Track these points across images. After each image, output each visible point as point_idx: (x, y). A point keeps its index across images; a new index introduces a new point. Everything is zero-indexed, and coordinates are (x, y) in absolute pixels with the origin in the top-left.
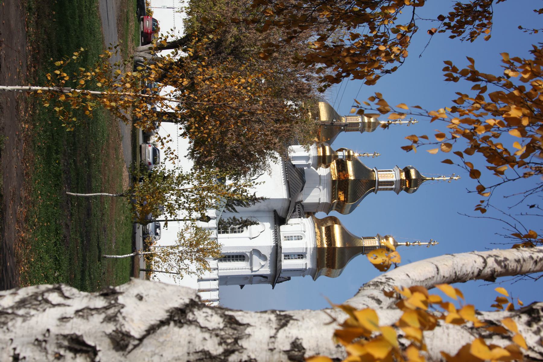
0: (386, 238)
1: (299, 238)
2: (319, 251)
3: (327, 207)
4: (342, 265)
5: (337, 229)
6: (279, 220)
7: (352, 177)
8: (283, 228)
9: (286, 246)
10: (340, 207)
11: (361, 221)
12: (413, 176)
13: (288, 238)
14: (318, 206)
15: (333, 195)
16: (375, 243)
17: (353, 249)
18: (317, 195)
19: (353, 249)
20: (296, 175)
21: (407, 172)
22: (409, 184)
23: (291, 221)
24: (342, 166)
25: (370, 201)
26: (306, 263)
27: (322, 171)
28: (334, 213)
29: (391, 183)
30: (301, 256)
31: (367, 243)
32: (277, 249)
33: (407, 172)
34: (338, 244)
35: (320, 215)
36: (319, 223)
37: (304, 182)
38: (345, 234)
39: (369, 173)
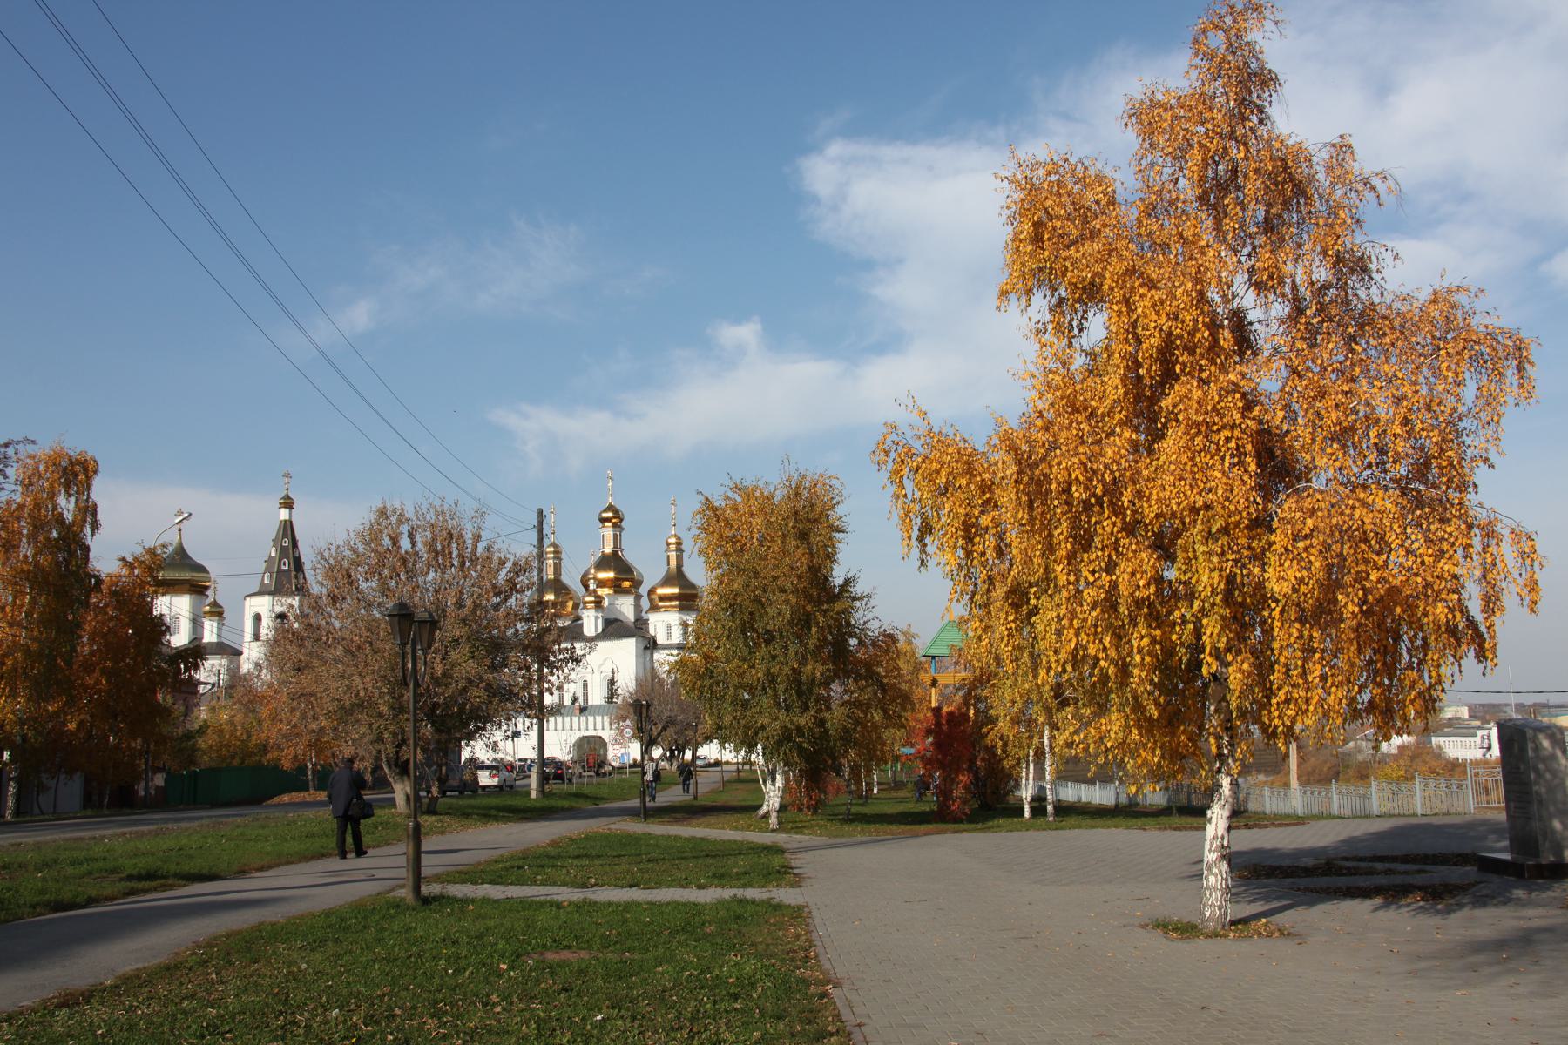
0: (668, 544)
1: (669, 628)
2: (682, 609)
3: (638, 597)
4: (693, 586)
5: (661, 591)
6: (651, 645)
7: (611, 575)
8: (659, 641)
9: (676, 637)
10: (637, 584)
11: (651, 569)
12: (610, 514)
13: (669, 635)
14: (638, 607)
15: (626, 592)
16: (673, 555)
17: (677, 577)
18: (626, 607)
19: (677, 577)
20: (610, 628)
21: (603, 520)
22: (616, 518)
23: (652, 632)
24: (601, 583)
25: (629, 555)
26: (690, 619)
27: (606, 603)
28: (644, 590)
29: (615, 536)
30: (685, 625)
31: (673, 563)
32: (680, 647)
33: (603, 520)
34: (676, 590)
35: (645, 603)
36: (654, 608)
37: (616, 620)
38: (667, 582)
39: (604, 556)
